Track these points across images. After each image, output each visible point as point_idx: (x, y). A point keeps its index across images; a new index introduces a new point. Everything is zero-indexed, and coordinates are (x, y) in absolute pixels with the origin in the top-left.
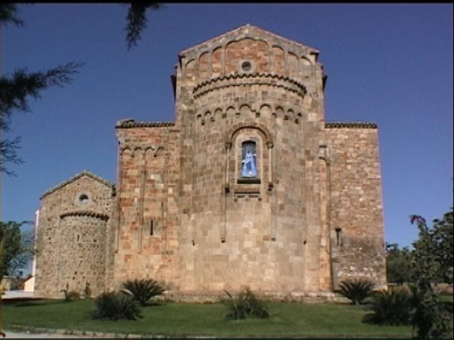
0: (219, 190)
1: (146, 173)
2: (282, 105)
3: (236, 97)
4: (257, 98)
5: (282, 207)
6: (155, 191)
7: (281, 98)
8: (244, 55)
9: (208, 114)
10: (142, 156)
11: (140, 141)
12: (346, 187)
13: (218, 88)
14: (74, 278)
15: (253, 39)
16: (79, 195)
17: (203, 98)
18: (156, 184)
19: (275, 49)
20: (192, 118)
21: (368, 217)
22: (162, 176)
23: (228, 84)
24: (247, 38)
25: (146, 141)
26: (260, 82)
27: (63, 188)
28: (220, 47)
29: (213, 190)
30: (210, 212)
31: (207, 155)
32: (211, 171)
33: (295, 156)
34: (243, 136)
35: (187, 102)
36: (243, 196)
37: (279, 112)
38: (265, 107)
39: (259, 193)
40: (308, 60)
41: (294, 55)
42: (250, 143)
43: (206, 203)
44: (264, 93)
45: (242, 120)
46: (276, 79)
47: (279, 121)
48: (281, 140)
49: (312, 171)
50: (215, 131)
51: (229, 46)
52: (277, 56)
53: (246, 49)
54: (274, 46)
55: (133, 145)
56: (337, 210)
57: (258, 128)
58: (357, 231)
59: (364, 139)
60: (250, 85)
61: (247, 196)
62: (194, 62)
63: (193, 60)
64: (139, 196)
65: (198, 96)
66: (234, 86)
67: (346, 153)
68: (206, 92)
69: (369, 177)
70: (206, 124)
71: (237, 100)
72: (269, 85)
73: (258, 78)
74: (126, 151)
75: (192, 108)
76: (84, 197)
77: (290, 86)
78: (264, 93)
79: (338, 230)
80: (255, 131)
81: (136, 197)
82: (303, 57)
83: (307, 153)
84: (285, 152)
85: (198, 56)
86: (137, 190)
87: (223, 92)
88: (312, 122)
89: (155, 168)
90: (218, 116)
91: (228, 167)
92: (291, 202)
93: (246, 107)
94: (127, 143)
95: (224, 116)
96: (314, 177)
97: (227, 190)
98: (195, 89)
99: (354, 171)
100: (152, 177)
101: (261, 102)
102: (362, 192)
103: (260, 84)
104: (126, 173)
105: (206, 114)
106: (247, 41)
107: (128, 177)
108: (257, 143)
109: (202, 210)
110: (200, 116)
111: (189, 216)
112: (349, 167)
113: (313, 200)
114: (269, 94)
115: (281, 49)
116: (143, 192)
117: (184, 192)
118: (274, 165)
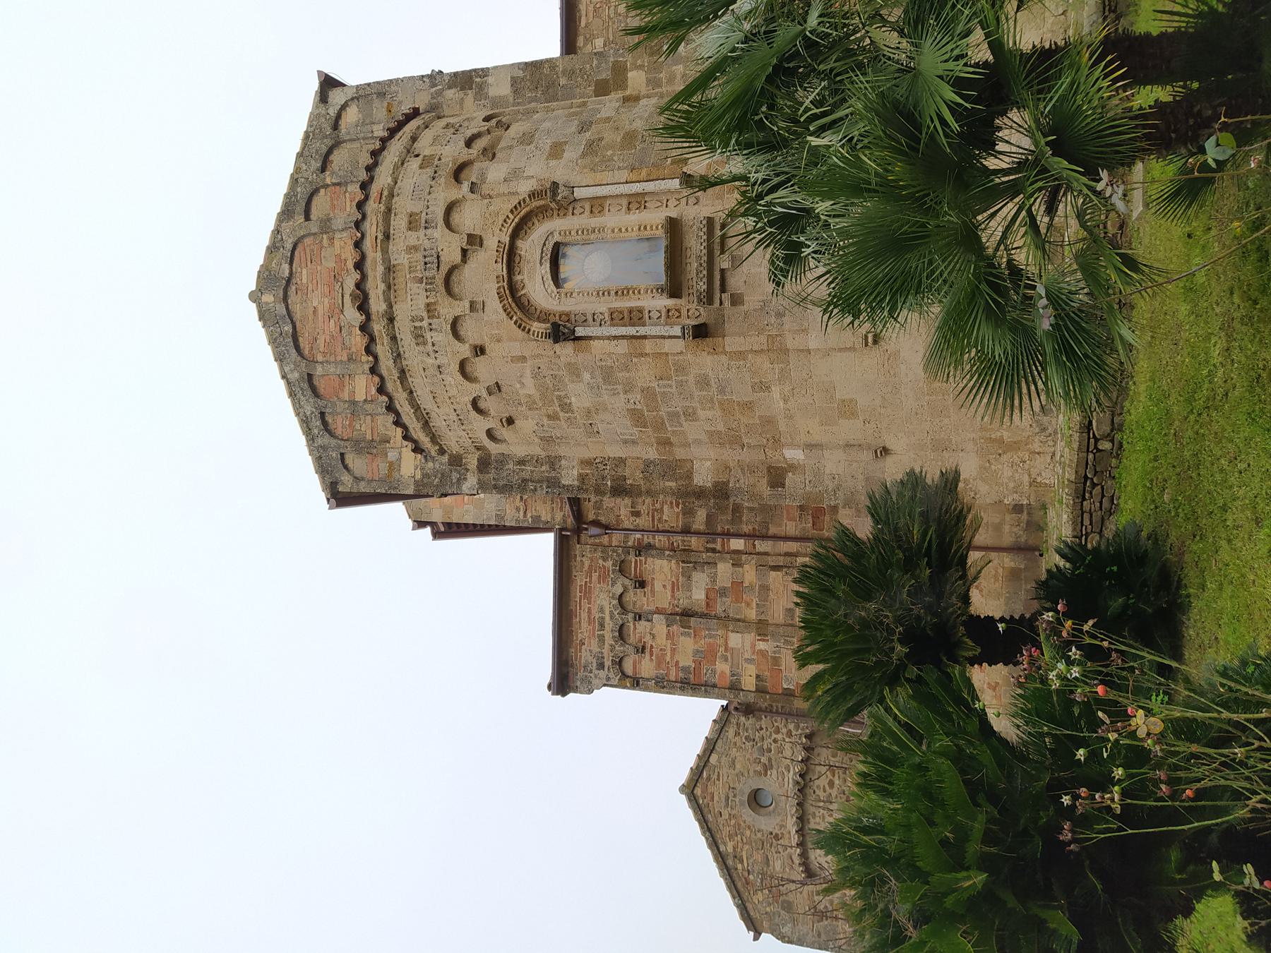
0: (704, 361)
1: (687, 614)
2: (451, 167)
3: (425, 314)
4: (427, 244)
6: (738, 585)
7: (430, 171)
9: (482, 405)
10: (643, 626)
11: (602, 626)
13: (403, 374)
15: (289, 281)
16: (747, 814)
17: (437, 422)
18: (719, 584)
19: (315, 213)
20: (503, 459)
22: (697, 565)
23: (386, 340)
25: (602, 610)
26: (380, 237)
27: (730, 862)
28: (310, 376)
29: (703, 382)
30: (776, 391)
31: (599, 408)
32: (648, 393)
34: (537, 287)
35: (455, 476)
37: (472, 175)
38: (456, 218)
39: (710, 221)
40: (344, 107)
41: (330, 151)
43: (748, 406)
44: (413, 224)
46: (375, 189)
47: (495, 172)
48: (553, 163)
50: (529, 380)
51: (306, 352)
52: (333, 207)
54: (307, 218)
55: (612, 648)
57: (515, 235)
60: (389, 269)
61: (724, 262)
62: (349, 459)
64: (750, 637)
65: (434, 439)
66: (391, 320)
68: (417, 408)
70: (512, 411)
71: (430, 308)
72: (389, 210)
74: (629, 670)
75: (472, 461)
76: (755, 799)
77: (396, 147)
78: (413, 224)
80: (523, 246)
81: (753, 646)
82: (336, 127)
83: (602, 89)
85: (333, 442)
86: (735, 640)
87: (414, 357)
89: (674, 587)
90: (480, 367)
91: (631, 331)
93: (454, 278)
94: (608, 663)
95: (480, 350)
97: (701, 332)
98: (417, 449)
100: (699, 595)
101: (439, 232)
103: (387, 237)
104: (685, 669)
105: (480, 411)
106: (293, 298)
107: (698, 664)
108: (557, 238)
109: (769, 421)
110: (490, 434)
111: (792, 467)
116: (740, 624)
117: (716, 484)
118: (624, 175)
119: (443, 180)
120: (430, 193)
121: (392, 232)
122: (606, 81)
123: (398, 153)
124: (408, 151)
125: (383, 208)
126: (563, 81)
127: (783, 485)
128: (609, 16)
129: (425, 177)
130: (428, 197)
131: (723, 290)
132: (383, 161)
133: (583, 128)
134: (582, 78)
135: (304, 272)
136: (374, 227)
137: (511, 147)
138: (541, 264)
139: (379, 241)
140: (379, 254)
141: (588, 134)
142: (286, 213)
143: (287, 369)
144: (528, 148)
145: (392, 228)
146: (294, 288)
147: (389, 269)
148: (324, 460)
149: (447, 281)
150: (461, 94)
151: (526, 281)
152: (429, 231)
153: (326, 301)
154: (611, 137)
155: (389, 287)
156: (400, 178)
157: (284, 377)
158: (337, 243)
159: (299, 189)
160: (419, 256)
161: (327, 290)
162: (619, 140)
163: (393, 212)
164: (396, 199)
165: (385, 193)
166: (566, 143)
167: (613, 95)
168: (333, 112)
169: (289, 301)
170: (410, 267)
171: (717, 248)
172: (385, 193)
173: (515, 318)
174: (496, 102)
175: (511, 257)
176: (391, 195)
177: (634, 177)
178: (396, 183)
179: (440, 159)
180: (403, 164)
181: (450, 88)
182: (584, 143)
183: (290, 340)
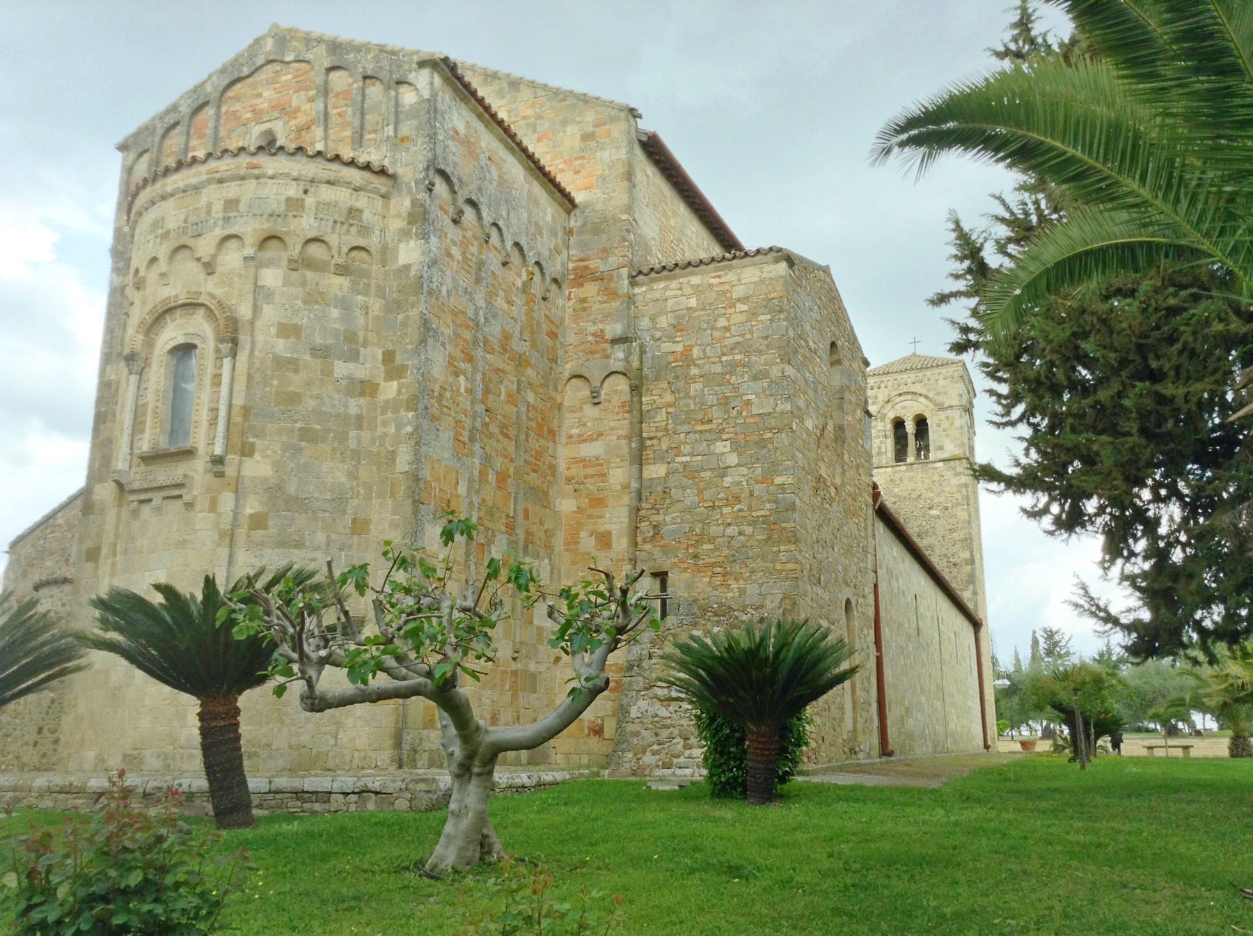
5: (258, 522)
8: (261, 111)
12: (686, 449)
14: (35, 744)
21: (748, 530)
24: (270, 62)
26: (218, 176)
33: (327, 372)
34: (171, 335)
36: (150, 500)
42: (185, 350)
44: (231, 204)
45: (175, 291)
48: (273, 330)
49: (396, 411)
51: (230, 94)
53: (265, 94)
56: (656, 518)
58: (714, 575)
59: (744, 300)
60: (197, 188)
61: (157, 498)
62: (146, 158)
63: (146, 151)
66: (163, 198)
67: (688, 349)
69: (755, 411)
72: (243, 178)
73: (212, 164)
78: (231, 204)
79: (661, 576)
83: (389, 357)
84: (291, 364)
85: (157, 139)
88: (407, 267)
92: (297, 504)
96: (399, 427)
99: (711, 399)
101: (219, 232)
102: (732, 459)
103: (221, 181)
112: (695, 388)
113: (393, 495)
114: (243, 206)
115: (308, 62)
118: (239, 400)
119: (266, 226)
120: (255, 215)
121: (226, 185)
122: (393, 361)
123: (303, 173)
124: (312, 181)
125: (242, 172)
126: (400, 317)
127: (87, 561)
129: (274, 206)
130: (250, 215)
131: (142, 502)
132: (294, 161)
133: (316, 351)
134: (400, 336)
135: (290, 77)
136: (225, 168)
137: (304, 283)
139: (215, 175)
141: (308, 357)
143: (215, 79)
144: (299, 303)
145: (228, 184)
146: (279, 68)
149: (185, 247)
150: (405, 215)
151: (175, 323)
152: (220, 222)
153: (266, 105)
154: (295, 382)
155: (184, 191)
157: (210, 77)
158: (308, 106)
159: (352, 56)
160: (203, 216)
161: (274, 103)
162: (290, 389)
163: (243, 182)
164: (254, 181)
165: (256, 172)
166: (299, 338)
167: (383, 368)
168: (411, 77)
169: (269, 66)
170: (196, 209)
171: (166, 493)
172: (256, 172)
174: (386, 253)
175: (191, 306)
176: (257, 177)
177: (235, 411)
179: (295, 216)
180: (295, 180)
182: (295, 356)
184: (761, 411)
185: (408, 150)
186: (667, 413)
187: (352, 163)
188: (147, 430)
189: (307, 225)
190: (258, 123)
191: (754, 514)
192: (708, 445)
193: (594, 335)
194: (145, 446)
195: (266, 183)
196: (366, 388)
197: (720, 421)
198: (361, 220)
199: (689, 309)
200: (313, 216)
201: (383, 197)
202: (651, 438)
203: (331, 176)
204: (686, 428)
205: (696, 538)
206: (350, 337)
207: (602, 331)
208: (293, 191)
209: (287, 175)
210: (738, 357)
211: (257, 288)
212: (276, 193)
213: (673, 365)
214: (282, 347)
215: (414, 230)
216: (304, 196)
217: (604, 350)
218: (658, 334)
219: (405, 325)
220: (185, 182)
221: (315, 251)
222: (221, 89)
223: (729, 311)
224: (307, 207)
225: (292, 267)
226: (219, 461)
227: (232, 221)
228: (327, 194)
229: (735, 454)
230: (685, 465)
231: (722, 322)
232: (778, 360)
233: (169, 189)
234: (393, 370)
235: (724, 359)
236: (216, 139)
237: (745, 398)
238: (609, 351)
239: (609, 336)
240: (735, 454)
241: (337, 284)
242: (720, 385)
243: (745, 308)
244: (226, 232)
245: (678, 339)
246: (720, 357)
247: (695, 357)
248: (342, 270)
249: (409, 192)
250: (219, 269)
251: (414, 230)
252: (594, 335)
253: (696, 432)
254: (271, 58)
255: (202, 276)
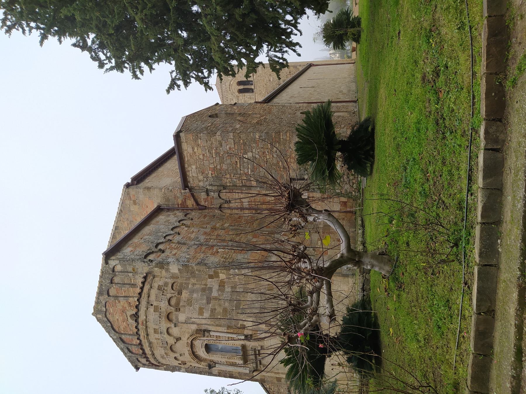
7: (158, 313)
21: (275, 149)
26: (145, 336)
27: (268, 390)
33: (216, 299)
34: (201, 352)
42: (208, 348)
44: (156, 331)
45: (186, 350)
51: (117, 330)
60: (150, 343)
62: (140, 359)
66: (153, 354)
72: (147, 327)
73: (142, 338)
78: (156, 331)
83: (211, 277)
84: (213, 310)
85: (133, 355)
88: (179, 270)
101: (166, 336)
103: (148, 335)
114: (157, 327)
115: (106, 303)
119: (163, 319)
120: (160, 323)
121: (149, 333)
122: (212, 275)
124: (148, 303)
125: (144, 327)
126: (197, 272)
127: (281, 381)
128: (196, 159)
129: (157, 316)
130: (160, 325)
131: (260, 364)
132: (140, 309)
133: (208, 303)
134: (204, 273)
135: (111, 309)
136: (143, 333)
137: (184, 306)
138: (202, 348)
140: (146, 340)
141: (210, 305)
142: (100, 293)
143: (111, 335)
144: (191, 308)
145: (149, 332)
146: (108, 313)
147: (150, 343)
148: (131, 359)
150: (161, 270)
152: (162, 335)
153: (121, 318)
154: (219, 310)
156: (148, 314)
157: (111, 337)
159: (103, 287)
160: (160, 341)
162: (221, 311)
163: (148, 327)
165: (144, 322)
167: (215, 279)
168: (111, 267)
172: (144, 322)
173: (196, 361)
174: (173, 276)
175: (192, 346)
177: (229, 331)
178: (147, 317)
179: (160, 309)
180: (147, 309)
181: (156, 267)
182: (210, 310)
183: (111, 328)
184: (233, 144)
185: (137, 269)
186: (233, 177)
187: (142, 288)
188: (235, 361)
189: (164, 305)
190: (128, 320)
191: (269, 147)
192: (245, 163)
193: (205, 202)
194: (241, 362)
195: (148, 319)
196: (222, 284)
197: (236, 158)
198: (162, 286)
199: (196, 168)
200: (161, 303)
201: (154, 278)
202: (242, 183)
203: (146, 296)
204: (239, 170)
205: (277, 168)
206: (204, 290)
207: (204, 199)
208: (151, 309)
209: (146, 311)
210: (214, 151)
211: (186, 322)
212: (152, 316)
213: (216, 174)
214: (207, 314)
215: (166, 267)
216: (153, 306)
217: (211, 199)
218: (205, 179)
219: (200, 271)
220: (148, 347)
221: (173, 302)
222: (115, 333)
223: (197, 154)
224: (157, 305)
225: (178, 310)
226: (246, 336)
227: (162, 331)
228: (153, 298)
229: (248, 153)
230: (252, 171)
231: (201, 157)
232: (215, 137)
233: (150, 353)
234: (216, 275)
235: (214, 156)
236: (132, 335)
237: (228, 150)
238: (211, 197)
239: (206, 197)
240: (248, 153)
241: (185, 295)
242: (224, 158)
243: (196, 148)
244: (166, 333)
245: (207, 173)
246: (214, 158)
247: (213, 167)
248: (180, 293)
249: (152, 268)
250: (179, 336)
251: (166, 267)
252: (205, 202)
253: (240, 167)
254: (104, 315)
255: (181, 341)
